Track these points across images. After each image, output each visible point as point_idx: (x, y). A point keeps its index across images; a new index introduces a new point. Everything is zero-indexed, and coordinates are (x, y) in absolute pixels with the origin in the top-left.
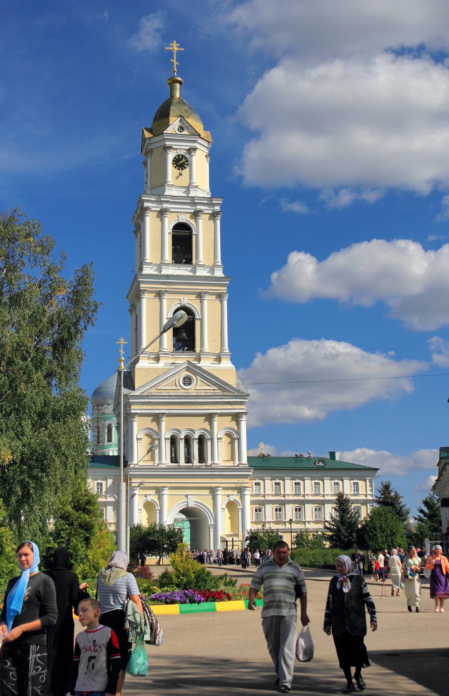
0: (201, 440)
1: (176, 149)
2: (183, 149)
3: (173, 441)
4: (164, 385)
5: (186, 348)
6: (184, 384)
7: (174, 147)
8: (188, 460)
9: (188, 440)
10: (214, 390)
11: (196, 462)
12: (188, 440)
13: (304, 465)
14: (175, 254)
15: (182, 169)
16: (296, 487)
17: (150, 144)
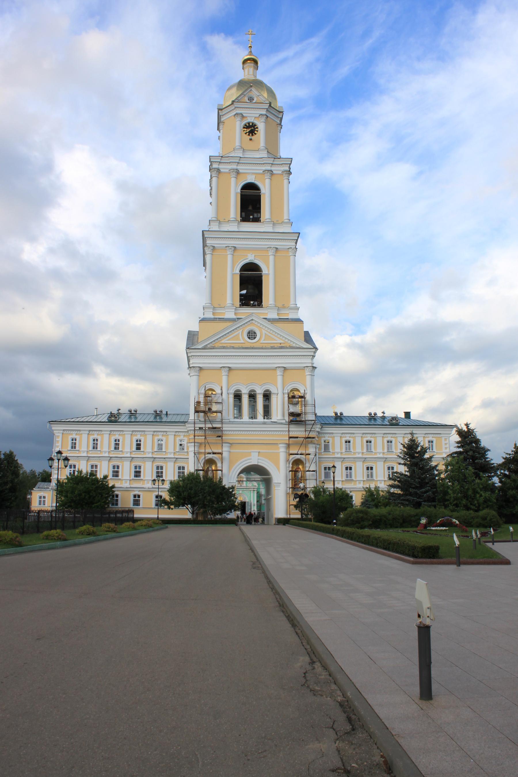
0: (267, 396)
1: (246, 117)
2: (252, 117)
3: (238, 396)
4: (227, 339)
5: (252, 302)
6: (249, 338)
7: (244, 115)
8: (253, 416)
9: (252, 396)
10: (280, 344)
11: (260, 418)
12: (252, 396)
13: (379, 422)
14: (243, 214)
15: (252, 135)
16: (367, 445)
17: (223, 115)
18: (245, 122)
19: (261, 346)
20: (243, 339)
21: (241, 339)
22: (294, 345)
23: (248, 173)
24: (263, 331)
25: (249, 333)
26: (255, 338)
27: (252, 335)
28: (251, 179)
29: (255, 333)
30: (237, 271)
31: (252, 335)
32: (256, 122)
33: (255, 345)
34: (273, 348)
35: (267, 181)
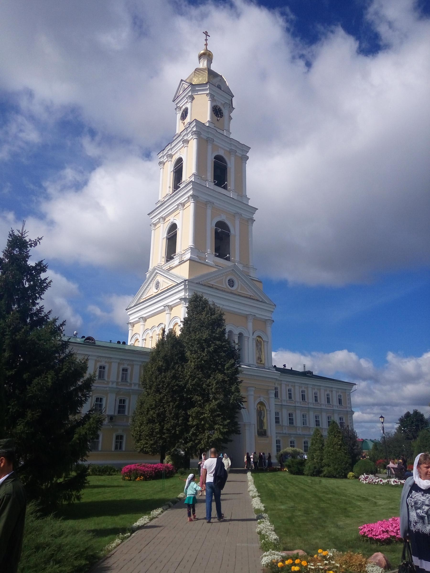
18: (215, 104)
19: (238, 293)
20: (225, 285)
21: (224, 284)
22: (259, 299)
23: (221, 148)
24: (240, 282)
25: (229, 280)
26: (233, 286)
27: (231, 283)
28: (221, 153)
29: (233, 282)
30: (214, 225)
31: (231, 283)
32: (222, 108)
33: (235, 292)
34: (246, 297)
35: (233, 159)
